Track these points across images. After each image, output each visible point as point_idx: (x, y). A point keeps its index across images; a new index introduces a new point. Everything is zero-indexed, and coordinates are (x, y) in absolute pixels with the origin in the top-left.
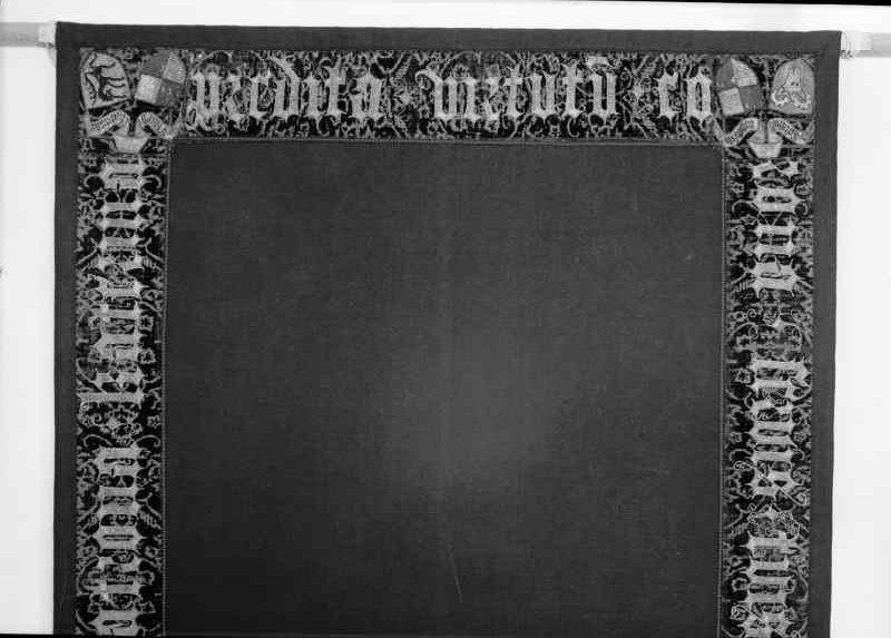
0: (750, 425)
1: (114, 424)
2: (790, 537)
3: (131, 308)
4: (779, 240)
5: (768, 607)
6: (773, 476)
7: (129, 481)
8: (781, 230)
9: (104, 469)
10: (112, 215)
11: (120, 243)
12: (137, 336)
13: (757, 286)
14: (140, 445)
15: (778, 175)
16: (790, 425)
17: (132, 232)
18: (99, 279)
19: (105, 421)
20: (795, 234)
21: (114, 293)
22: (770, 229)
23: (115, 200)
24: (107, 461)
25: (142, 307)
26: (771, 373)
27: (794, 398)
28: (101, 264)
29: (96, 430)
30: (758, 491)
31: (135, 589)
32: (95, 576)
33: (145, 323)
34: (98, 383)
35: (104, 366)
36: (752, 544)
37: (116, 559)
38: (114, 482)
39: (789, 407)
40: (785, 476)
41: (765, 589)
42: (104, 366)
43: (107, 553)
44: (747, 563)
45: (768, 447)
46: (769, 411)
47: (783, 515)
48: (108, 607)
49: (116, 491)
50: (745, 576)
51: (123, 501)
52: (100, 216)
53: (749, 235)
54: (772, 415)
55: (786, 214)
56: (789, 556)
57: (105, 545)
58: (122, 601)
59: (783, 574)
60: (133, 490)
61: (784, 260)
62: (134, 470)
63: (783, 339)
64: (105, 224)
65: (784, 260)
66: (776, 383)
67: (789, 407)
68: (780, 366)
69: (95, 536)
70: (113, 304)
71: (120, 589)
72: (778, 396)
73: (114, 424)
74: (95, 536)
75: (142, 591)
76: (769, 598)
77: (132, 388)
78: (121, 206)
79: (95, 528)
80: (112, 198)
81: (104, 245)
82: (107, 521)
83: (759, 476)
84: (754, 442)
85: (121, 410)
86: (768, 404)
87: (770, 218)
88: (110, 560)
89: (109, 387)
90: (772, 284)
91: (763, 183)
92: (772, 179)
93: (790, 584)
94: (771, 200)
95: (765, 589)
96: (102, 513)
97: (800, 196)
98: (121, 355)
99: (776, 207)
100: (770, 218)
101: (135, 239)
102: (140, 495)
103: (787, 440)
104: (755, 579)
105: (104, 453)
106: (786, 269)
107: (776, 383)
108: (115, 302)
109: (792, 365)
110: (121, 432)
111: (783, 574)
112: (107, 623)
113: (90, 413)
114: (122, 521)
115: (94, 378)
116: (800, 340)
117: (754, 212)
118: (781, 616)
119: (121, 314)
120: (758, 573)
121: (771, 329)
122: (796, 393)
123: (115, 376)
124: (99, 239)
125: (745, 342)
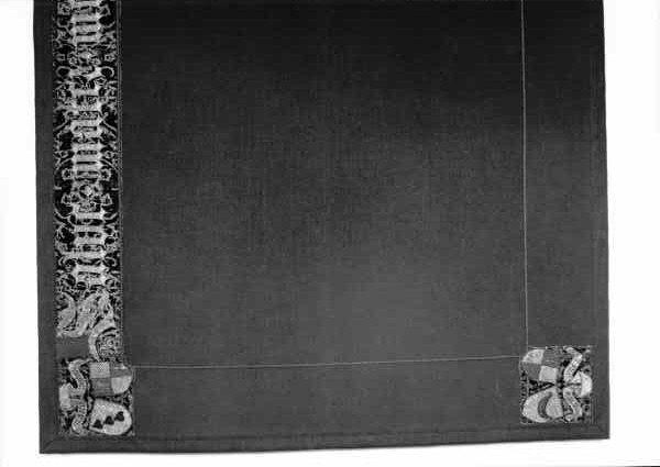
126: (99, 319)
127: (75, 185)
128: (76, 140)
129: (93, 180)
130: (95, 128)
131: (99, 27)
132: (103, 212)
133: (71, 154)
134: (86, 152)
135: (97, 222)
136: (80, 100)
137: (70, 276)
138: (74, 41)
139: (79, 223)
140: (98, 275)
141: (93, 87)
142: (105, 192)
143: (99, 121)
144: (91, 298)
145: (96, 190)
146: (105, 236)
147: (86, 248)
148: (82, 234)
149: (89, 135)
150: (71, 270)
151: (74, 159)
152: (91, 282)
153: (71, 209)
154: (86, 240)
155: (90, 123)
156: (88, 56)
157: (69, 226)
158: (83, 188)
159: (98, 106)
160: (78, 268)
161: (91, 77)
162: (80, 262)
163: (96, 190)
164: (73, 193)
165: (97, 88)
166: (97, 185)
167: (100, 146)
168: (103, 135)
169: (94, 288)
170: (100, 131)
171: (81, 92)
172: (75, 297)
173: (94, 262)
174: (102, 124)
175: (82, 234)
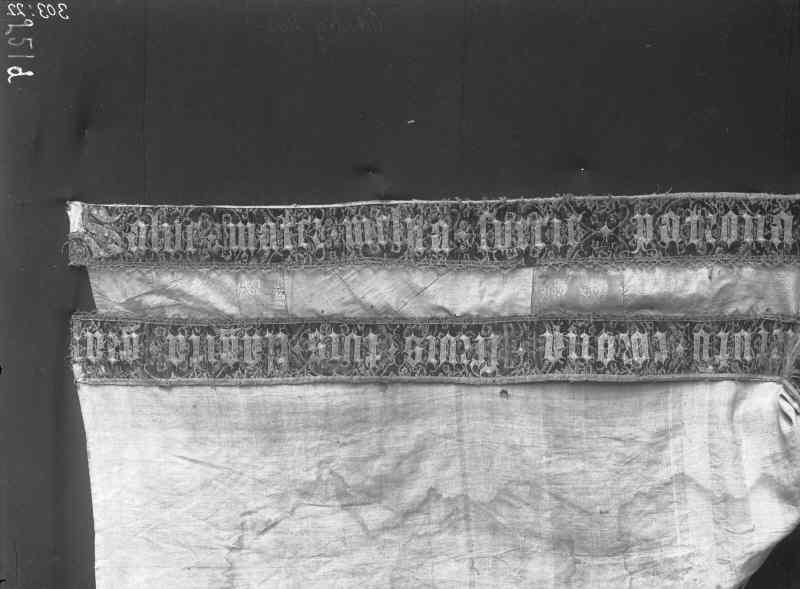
0: (453, 335)
2: (377, 362)
4: (579, 350)
5: (328, 349)
6: (418, 350)
8: (585, 351)
13: (547, 334)
15: (623, 350)
16: (453, 362)
20: (583, 360)
22: (586, 342)
26: (488, 349)
27: (472, 365)
30: (408, 339)
36: (372, 336)
39: (465, 362)
40: (418, 360)
41: (341, 346)
44: (359, 334)
45: (438, 346)
46: (462, 348)
47: (392, 358)
50: (350, 332)
53: (580, 330)
54: (460, 349)
55: (596, 355)
56: (364, 362)
59: (352, 358)
61: (565, 353)
63: (512, 356)
65: (565, 353)
66: (481, 351)
67: (465, 362)
68: (494, 351)
72: (473, 355)
76: (335, 347)
83: (418, 340)
84: (442, 337)
86: (467, 347)
87: (593, 344)
90: (548, 344)
91: (616, 341)
92: (619, 345)
93: (345, 363)
94: (606, 345)
95: (341, 346)
97: (609, 365)
99: (601, 348)
100: (593, 344)
103: (443, 360)
104: (347, 339)
106: (560, 355)
107: (481, 351)
109: (494, 363)
111: (352, 358)
116: (512, 367)
117: (598, 333)
118: (323, 357)
120: (352, 340)
121: (518, 346)
122: (475, 367)
125: (509, 329)
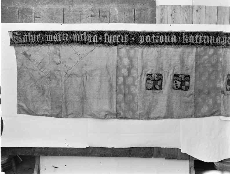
1: (179, 38)
3: (198, 41)
7: (170, 40)
9: (172, 37)
10: (212, 38)
11: (208, 40)
12: (193, 42)
14: (176, 42)
17: (210, 41)
18: (202, 36)
19: (180, 37)
21: (200, 39)
23: (215, 39)
24: (174, 37)
25: (198, 43)
28: (205, 37)
29: (178, 36)
31: (153, 42)
32: (156, 36)
33: (195, 43)
34: (186, 36)
35: (189, 37)
37: (158, 39)
38: (170, 38)
42: (189, 37)
43: (159, 37)
48: (151, 37)
49: (169, 38)
51: (167, 40)
52: (212, 36)
57: (160, 37)
58: (152, 40)
60: (169, 41)
62: (172, 41)
64: (211, 37)
69: (162, 35)
70: (198, 38)
71: (153, 39)
73: (179, 38)
74: (162, 35)
75: (153, 43)
77: (185, 41)
78: (214, 40)
79: (163, 35)
80: (215, 38)
81: (208, 37)
82: (164, 37)
85: (182, 39)
88: (158, 37)
89: (185, 37)
96: (165, 36)
98: (190, 40)
101: (209, 42)
102: (168, 42)
105: (175, 37)
108: (199, 39)
110: (178, 39)
112: (148, 37)
113: (181, 34)
114: (164, 40)
115: (187, 35)
119: (197, 39)
123: (187, 38)
124: (209, 36)
126: (16, 40)
127: (44, 35)
128: (53, 36)
129: (45, 39)
130: (56, 40)
131: (77, 40)
132: (38, 41)
133: (50, 34)
134: (51, 38)
135: (36, 40)
136: (61, 36)
137: (25, 34)
138: (73, 35)
139: (36, 36)
140: (25, 40)
141: (64, 39)
142: (43, 42)
143: (57, 40)
144: (20, 38)
145: (43, 40)
146: (33, 41)
147: (31, 38)
148: (34, 37)
149: (54, 38)
150: (26, 34)
151: (49, 35)
152: (24, 39)
153: (39, 34)
154: (32, 37)
155: (57, 38)
156: (71, 37)
157: (35, 34)
158: (43, 37)
159: (60, 40)
160: (26, 36)
161: (66, 38)
162: (28, 36)
163: (43, 40)
164: (42, 35)
165: (64, 40)
166: (44, 40)
167: (52, 41)
168: (54, 41)
169: (23, 39)
170: (55, 41)
171: (63, 36)
172: (21, 35)
173: (28, 39)
174: (56, 41)
175: (34, 37)
